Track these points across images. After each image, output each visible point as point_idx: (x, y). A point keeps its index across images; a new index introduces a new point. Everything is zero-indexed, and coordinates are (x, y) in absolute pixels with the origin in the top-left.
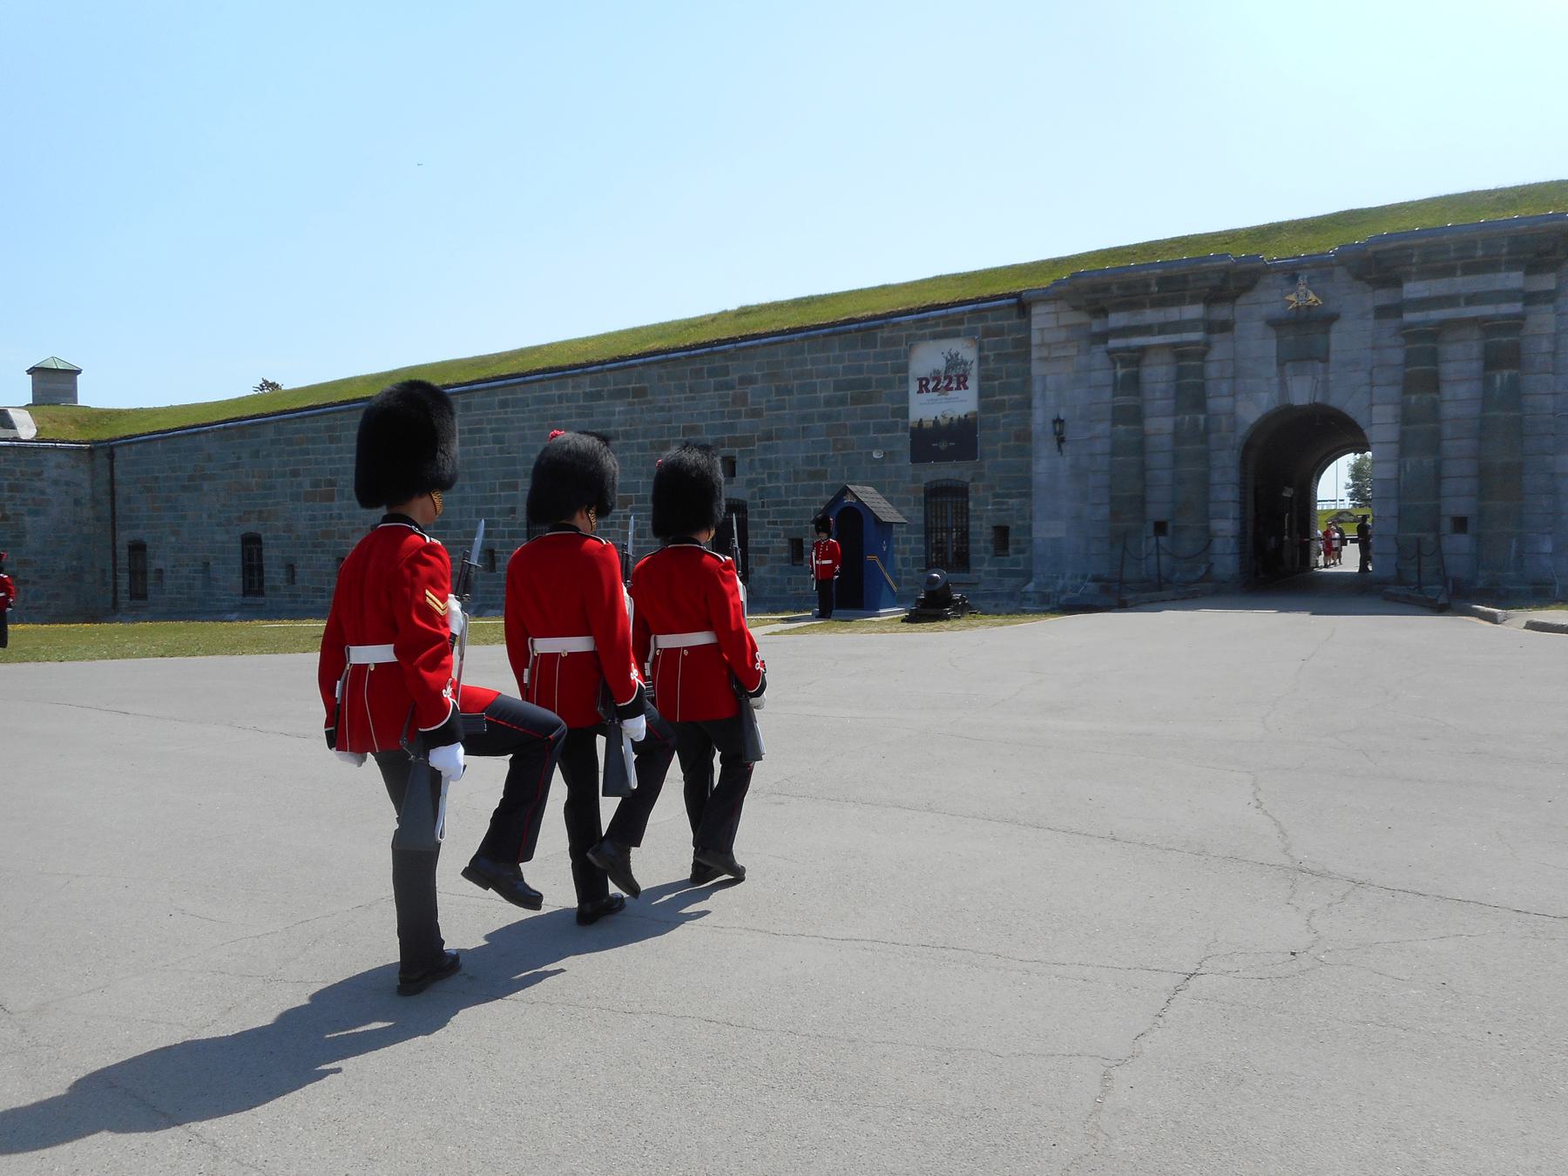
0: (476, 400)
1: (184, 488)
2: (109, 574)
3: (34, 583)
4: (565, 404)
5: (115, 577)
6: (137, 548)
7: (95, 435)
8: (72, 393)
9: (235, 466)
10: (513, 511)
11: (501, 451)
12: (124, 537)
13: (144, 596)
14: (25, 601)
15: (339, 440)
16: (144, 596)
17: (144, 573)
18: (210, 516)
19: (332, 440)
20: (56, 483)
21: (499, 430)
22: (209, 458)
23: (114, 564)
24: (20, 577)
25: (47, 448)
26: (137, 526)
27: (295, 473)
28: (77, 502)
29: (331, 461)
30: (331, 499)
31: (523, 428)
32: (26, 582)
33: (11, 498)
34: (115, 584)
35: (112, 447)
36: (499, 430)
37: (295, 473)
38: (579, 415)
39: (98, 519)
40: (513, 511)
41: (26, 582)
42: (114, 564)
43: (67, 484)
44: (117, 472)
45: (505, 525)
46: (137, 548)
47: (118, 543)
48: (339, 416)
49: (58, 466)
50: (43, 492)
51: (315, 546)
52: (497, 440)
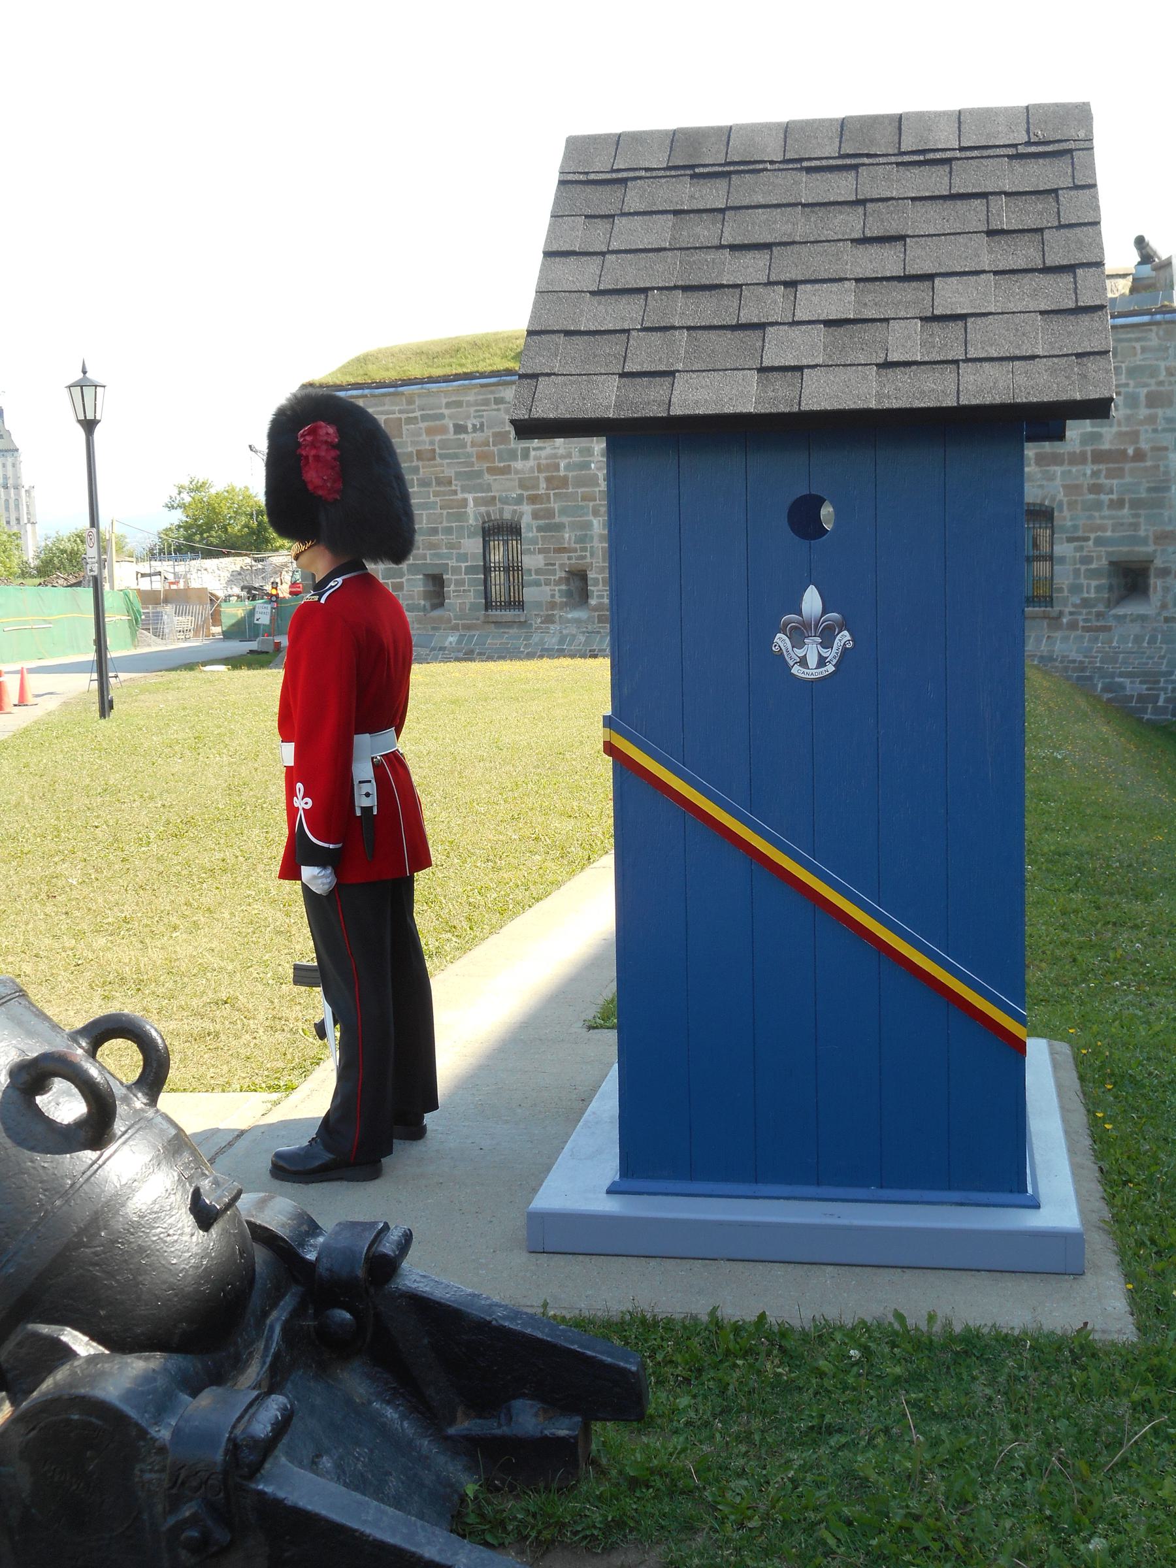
14: (1164, 606)
33: (1152, 419)
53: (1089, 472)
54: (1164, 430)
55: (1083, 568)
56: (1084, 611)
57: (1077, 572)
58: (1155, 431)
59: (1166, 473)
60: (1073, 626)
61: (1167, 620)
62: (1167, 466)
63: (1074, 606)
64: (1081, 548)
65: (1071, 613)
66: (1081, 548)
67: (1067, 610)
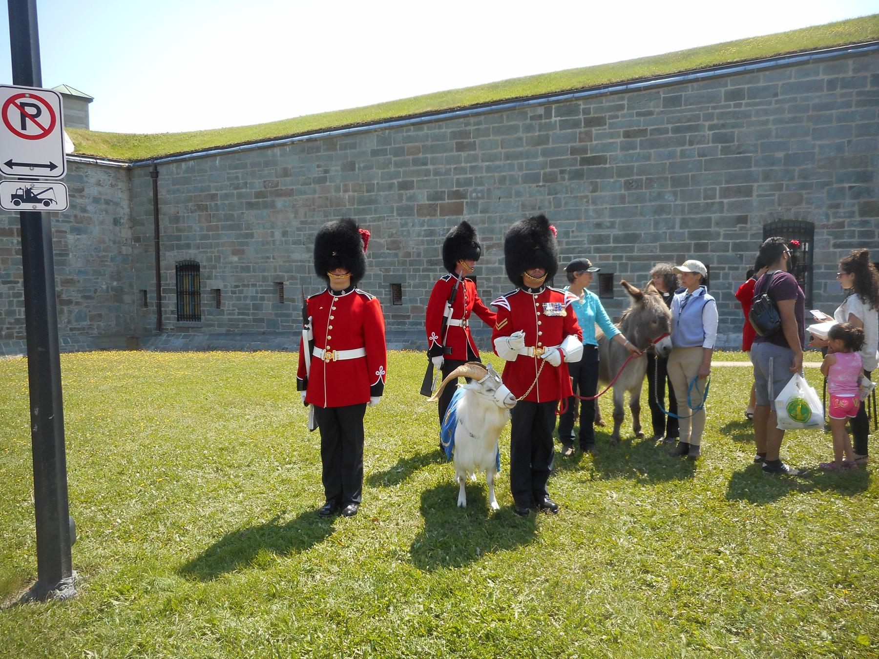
0: (690, 91)
1: (251, 206)
2: (152, 298)
3: (77, 303)
4: (839, 91)
5: (159, 298)
6: (188, 269)
7: (129, 155)
8: (84, 121)
9: (322, 180)
10: (743, 220)
11: (725, 150)
12: (171, 258)
13: (196, 317)
14: (69, 322)
15: (472, 146)
16: (196, 317)
17: (195, 294)
18: (285, 234)
19: (460, 147)
20: (96, 200)
21: (724, 126)
22: (286, 173)
23: (159, 285)
24: (64, 297)
25: (89, 164)
26: (188, 246)
27: (404, 186)
28: (116, 222)
29: (463, 170)
30: (459, 210)
31: (766, 122)
32: (69, 302)
34: (159, 306)
35: (156, 166)
36: (724, 126)
37: (404, 186)
38: (859, 104)
39: (137, 239)
40: (743, 220)
41: (69, 302)
42: (159, 285)
43: (107, 202)
44: (162, 193)
45: (727, 236)
46: (188, 269)
47: (162, 264)
48: (472, 120)
49: (98, 184)
50: (84, 210)
51: (431, 263)
52: (717, 139)
53: (15, 242)
54: (63, 221)
55: (15, 300)
56: (17, 327)
57: (10, 303)
58: (58, 221)
59: (66, 246)
60: (10, 336)
61: (71, 329)
62: (66, 242)
63: (10, 323)
64: (13, 288)
65: (8, 328)
66: (13, 288)
67: (5, 327)
